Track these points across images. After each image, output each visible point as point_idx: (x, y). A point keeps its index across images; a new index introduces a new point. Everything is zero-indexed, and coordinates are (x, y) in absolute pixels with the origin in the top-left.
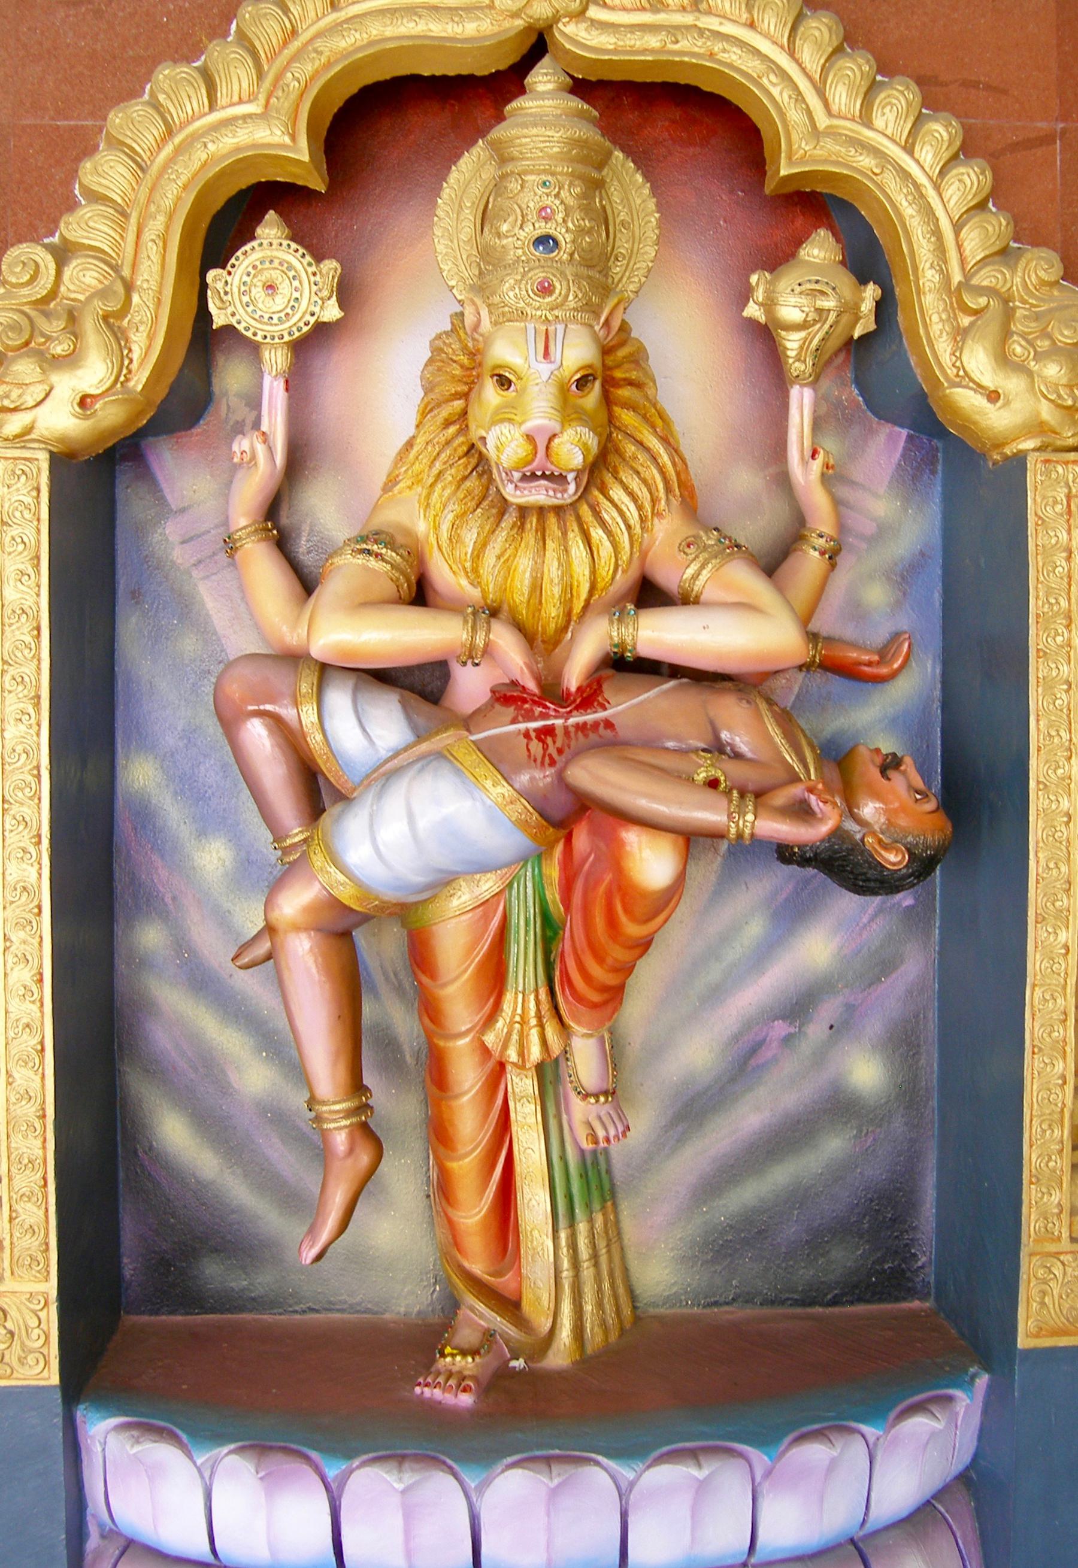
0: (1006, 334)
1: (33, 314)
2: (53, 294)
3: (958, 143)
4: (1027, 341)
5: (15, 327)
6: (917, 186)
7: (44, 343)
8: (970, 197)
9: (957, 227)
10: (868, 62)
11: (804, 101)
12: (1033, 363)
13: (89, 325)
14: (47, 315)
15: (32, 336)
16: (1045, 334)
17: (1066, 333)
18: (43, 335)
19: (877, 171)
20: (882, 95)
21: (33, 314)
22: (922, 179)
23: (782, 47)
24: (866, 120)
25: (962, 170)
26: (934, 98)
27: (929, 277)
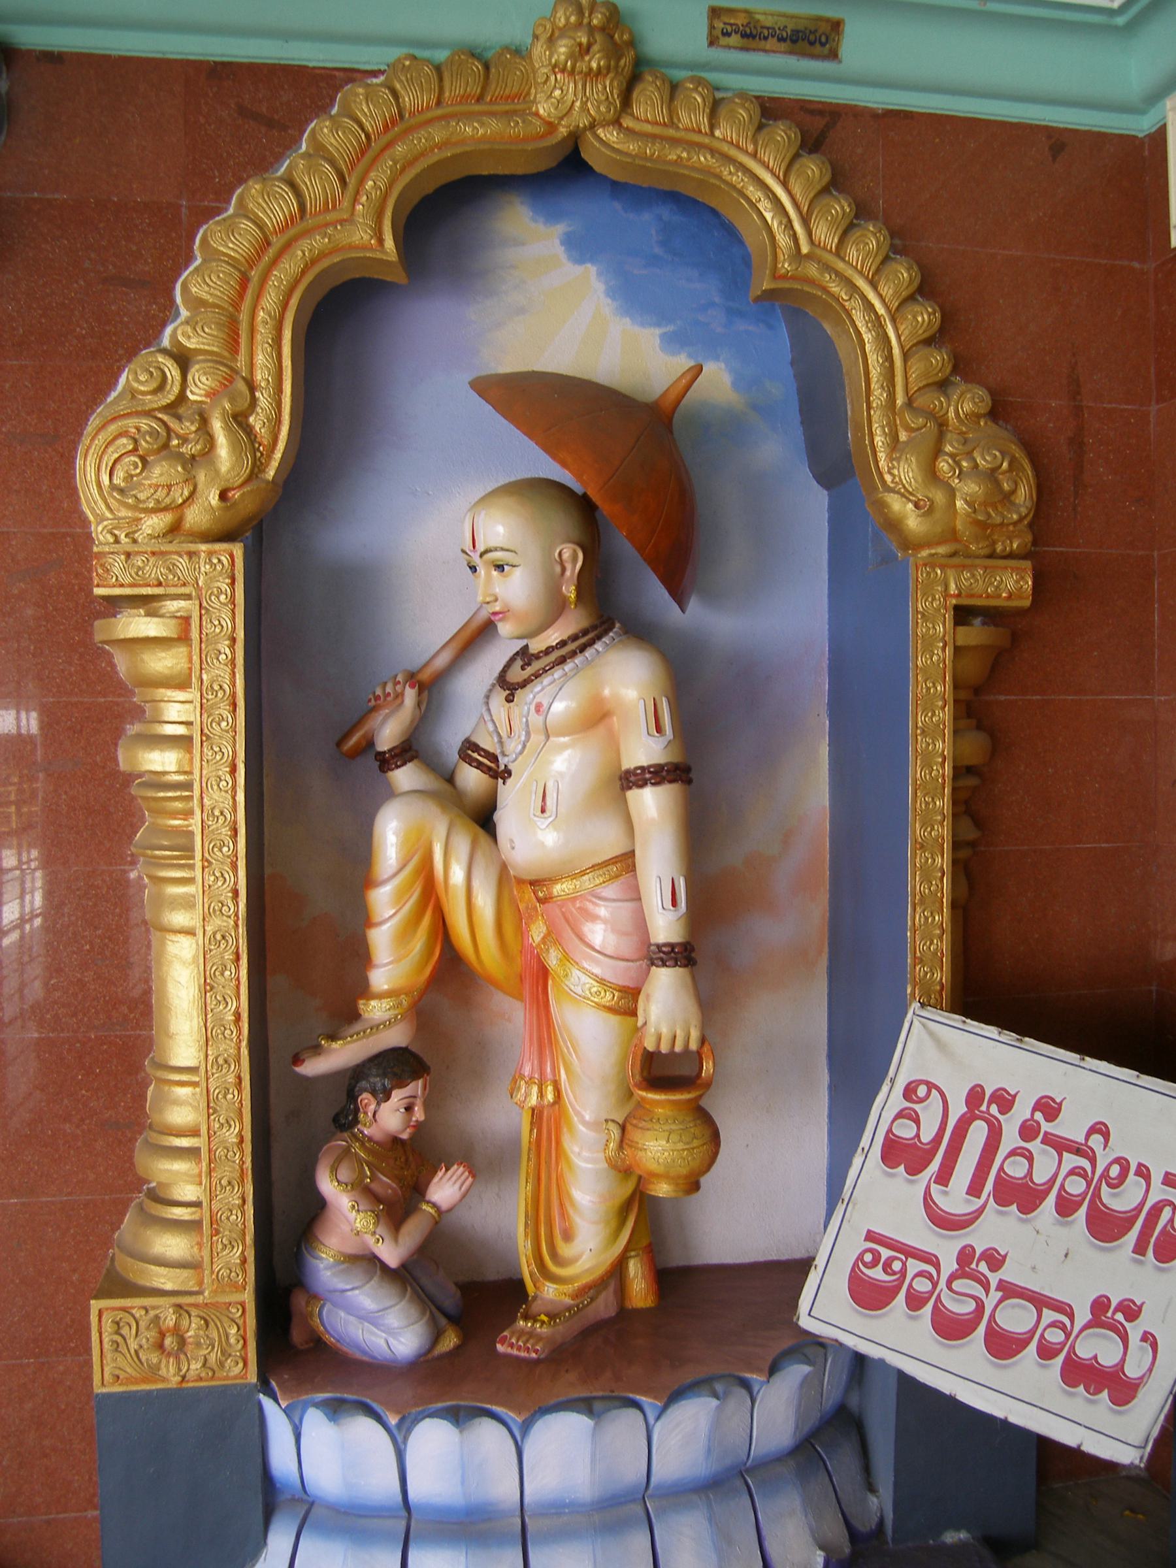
0: (938, 452)
1: (165, 418)
2: (182, 398)
3: (916, 284)
4: (954, 461)
5: (153, 433)
6: (878, 317)
7: (178, 446)
8: (921, 332)
9: (906, 356)
10: (849, 205)
11: (792, 227)
12: (957, 481)
13: (217, 426)
14: (179, 418)
15: (169, 438)
16: (969, 455)
17: (988, 458)
18: (178, 437)
19: (845, 297)
20: (858, 234)
21: (165, 418)
22: (881, 310)
23: (778, 177)
24: (839, 253)
25: (917, 308)
26: (901, 244)
27: (879, 395)
